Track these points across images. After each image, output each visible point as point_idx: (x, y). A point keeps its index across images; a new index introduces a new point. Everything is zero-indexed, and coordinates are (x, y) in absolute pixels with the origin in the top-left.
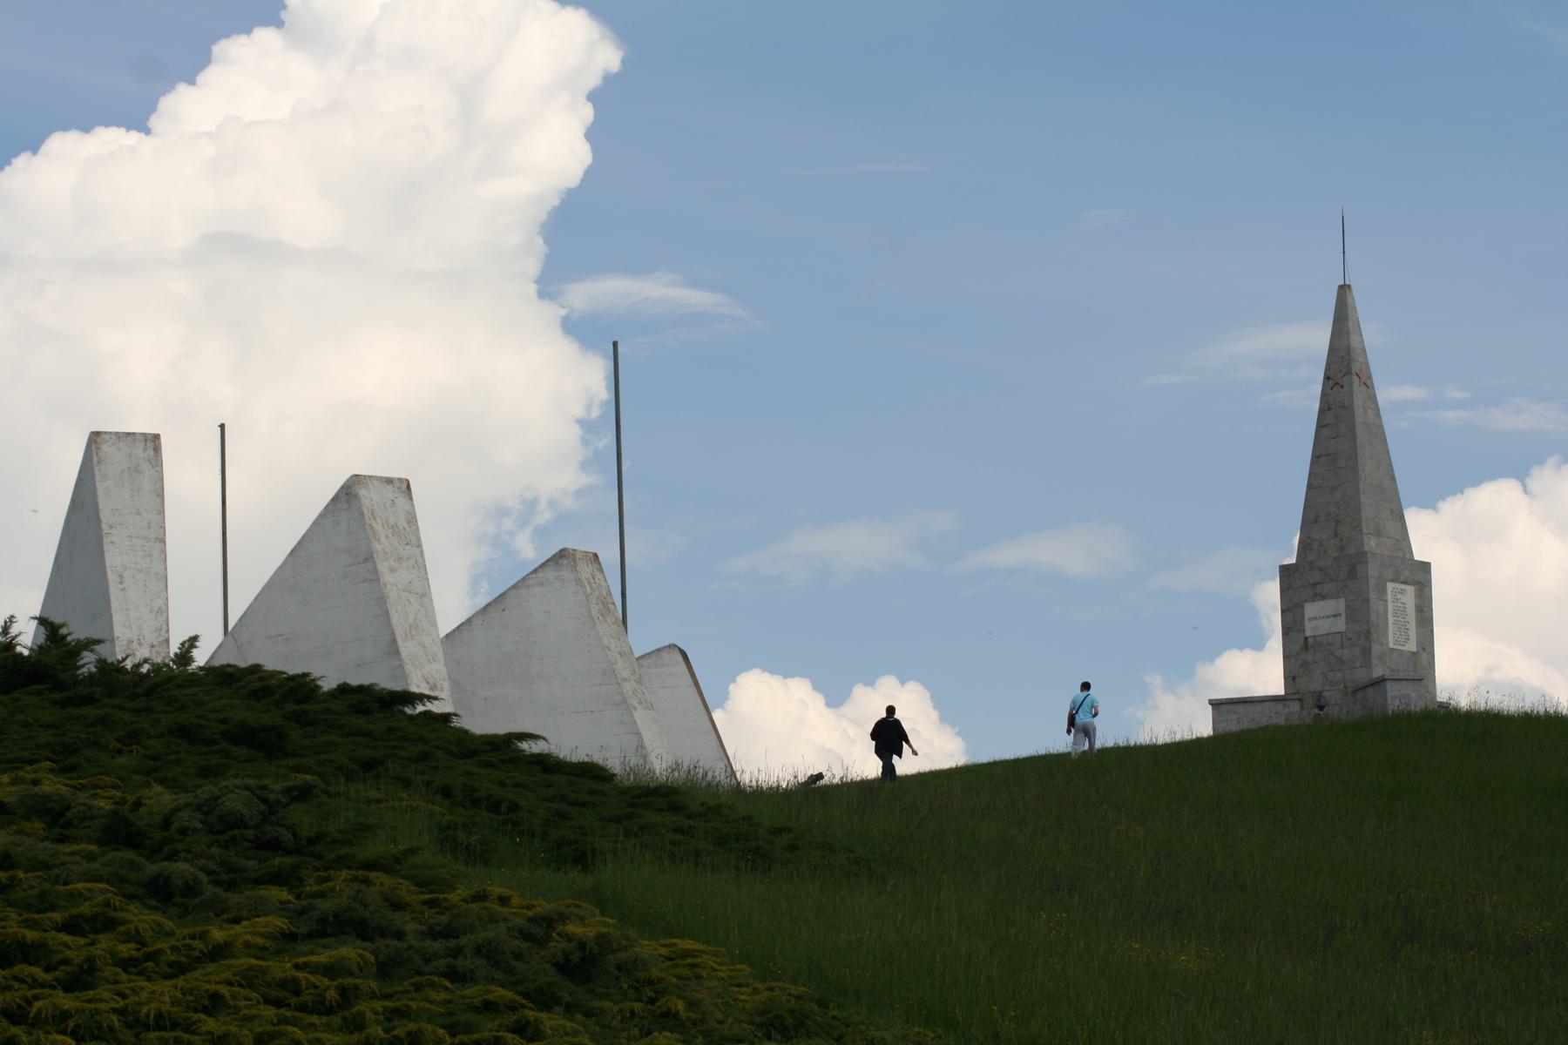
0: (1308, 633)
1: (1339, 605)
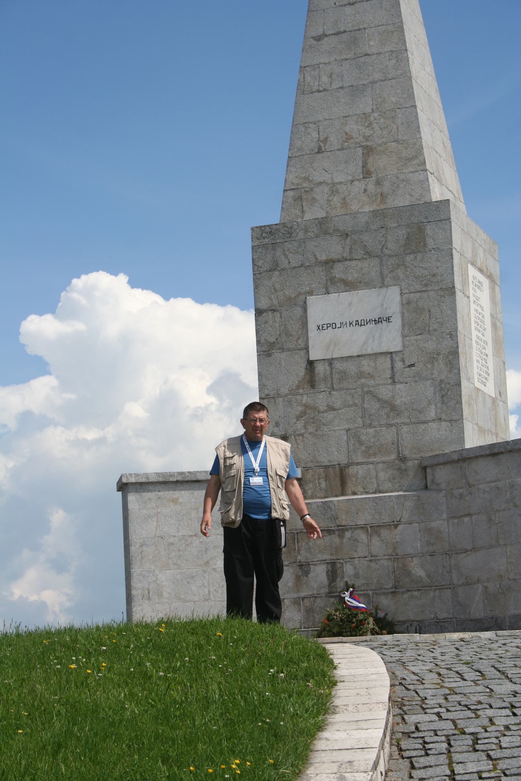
1: (391, 299)
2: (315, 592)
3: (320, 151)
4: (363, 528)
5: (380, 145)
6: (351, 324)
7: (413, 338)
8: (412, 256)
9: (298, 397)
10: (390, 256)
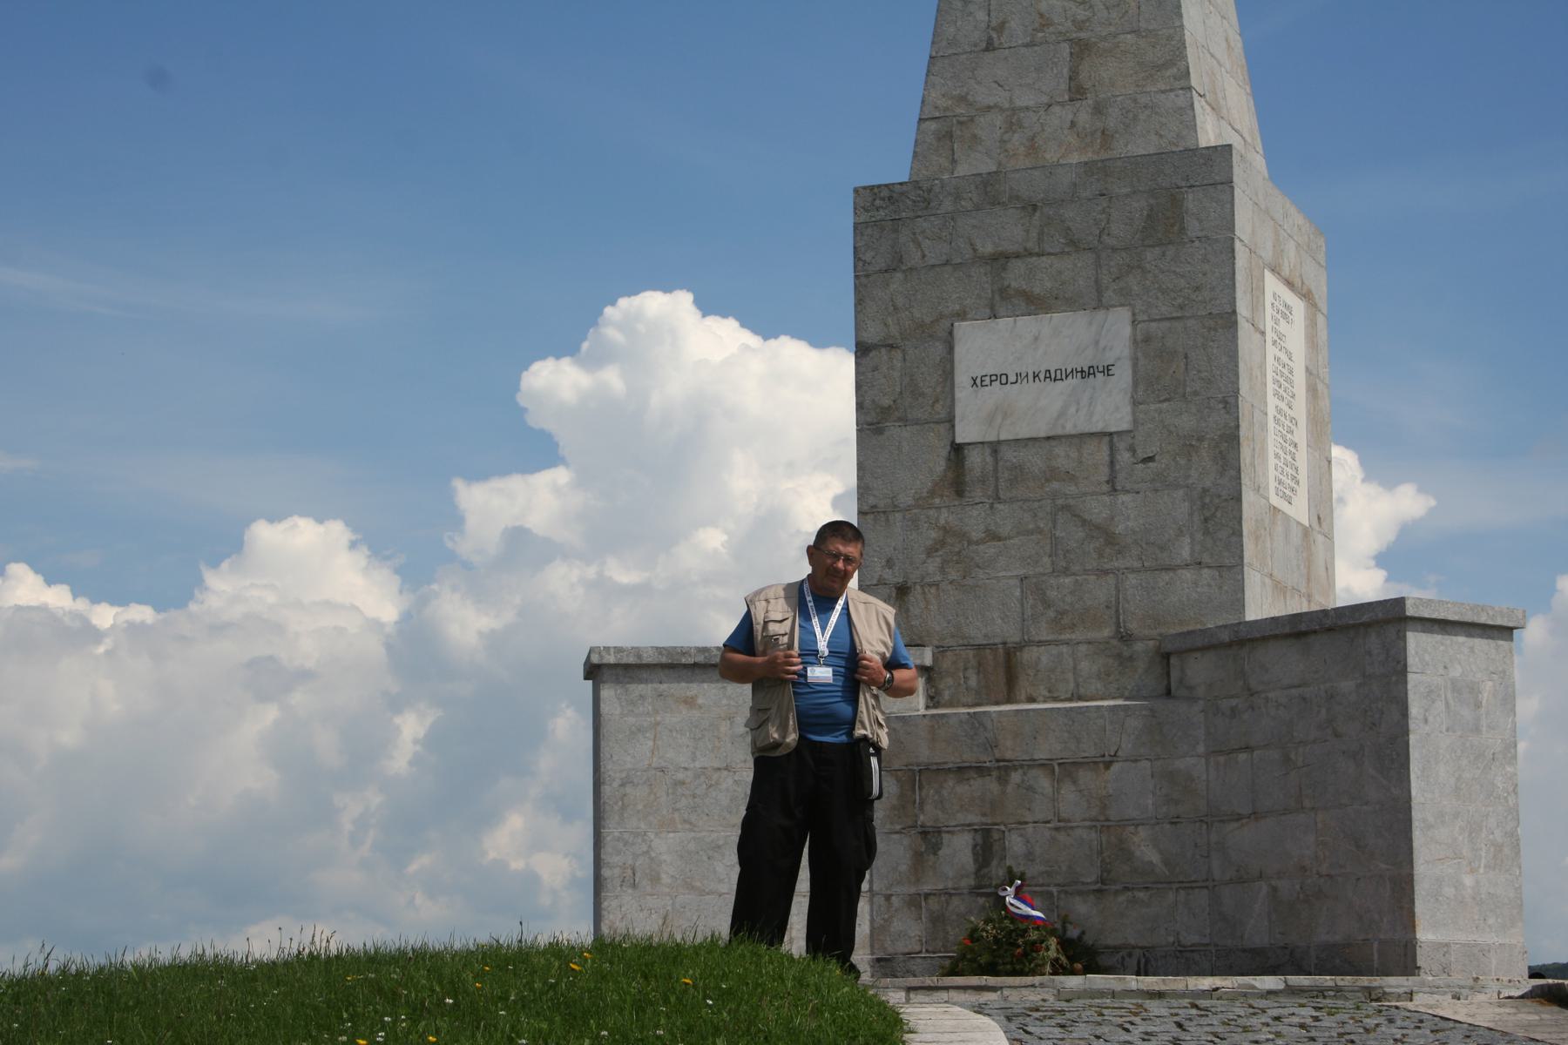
0: (966, 432)
1: (1114, 332)
2: (950, 885)
3: (990, 47)
4: (1046, 765)
5: (1105, 39)
6: (1036, 376)
7: (1153, 407)
8: (1157, 251)
9: (931, 512)
10: (1114, 250)
